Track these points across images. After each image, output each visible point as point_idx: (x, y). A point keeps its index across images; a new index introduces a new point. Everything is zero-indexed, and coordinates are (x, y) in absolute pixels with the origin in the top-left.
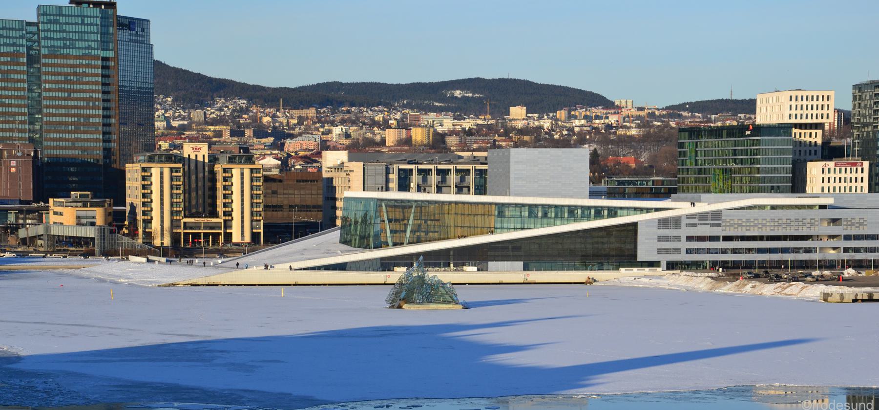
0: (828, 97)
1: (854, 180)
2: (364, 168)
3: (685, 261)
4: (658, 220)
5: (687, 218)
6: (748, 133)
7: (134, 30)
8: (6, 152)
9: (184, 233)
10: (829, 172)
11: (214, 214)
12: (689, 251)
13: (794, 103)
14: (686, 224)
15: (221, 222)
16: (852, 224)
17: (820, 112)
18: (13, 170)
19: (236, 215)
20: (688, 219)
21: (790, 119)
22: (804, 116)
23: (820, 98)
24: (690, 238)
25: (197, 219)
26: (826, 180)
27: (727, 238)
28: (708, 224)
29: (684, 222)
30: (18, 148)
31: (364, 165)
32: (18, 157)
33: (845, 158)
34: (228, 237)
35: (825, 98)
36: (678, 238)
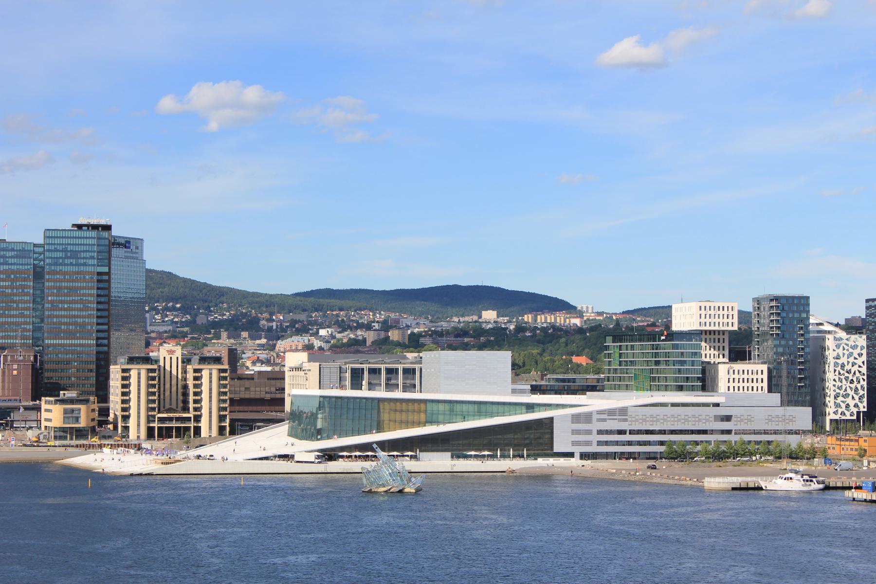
0: (732, 307)
1: (755, 381)
2: (320, 367)
3: (596, 452)
4: (572, 415)
5: (597, 414)
6: (663, 338)
7: (129, 248)
8: (9, 357)
9: (158, 427)
11: (186, 409)
12: (600, 443)
13: (703, 312)
14: (597, 419)
15: (191, 417)
16: (742, 421)
17: (725, 320)
18: (15, 372)
19: (205, 412)
20: (598, 415)
21: (700, 325)
22: (712, 324)
23: (726, 309)
24: (600, 432)
25: (169, 414)
26: (731, 380)
27: (632, 432)
28: (616, 419)
29: (595, 417)
30: (20, 353)
31: (320, 365)
32: (20, 361)
33: (747, 361)
34: (197, 431)
35: (730, 309)
36: (589, 432)
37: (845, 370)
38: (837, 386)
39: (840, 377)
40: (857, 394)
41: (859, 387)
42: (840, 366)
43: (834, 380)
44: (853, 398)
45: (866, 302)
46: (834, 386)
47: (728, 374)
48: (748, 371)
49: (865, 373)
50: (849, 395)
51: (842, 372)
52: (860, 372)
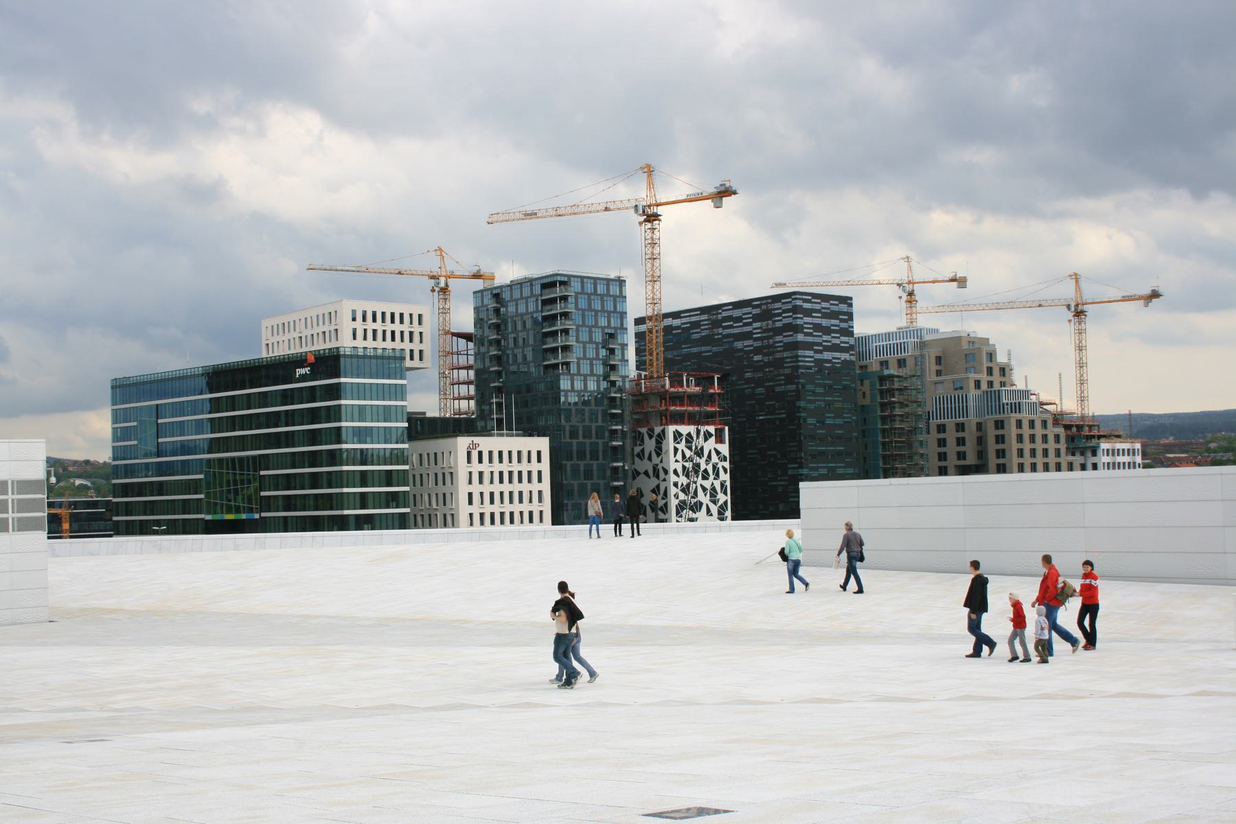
0: (420, 316)
10: (480, 461)
13: (359, 325)
26: (475, 477)
37: (694, 448)
38: (680, 485)
39: (685, 464)
40: (715, 502)
41: (717, 485)
42: (684, 440)
43: (675, 472)
44: (708, 511)
45: (636, 324)
46: (676, 485)
47: (469, 461)
48: (510, 452)
49: (728, 456)
50: (701, 504)
51: (688, 453)
52: (718, 453)
